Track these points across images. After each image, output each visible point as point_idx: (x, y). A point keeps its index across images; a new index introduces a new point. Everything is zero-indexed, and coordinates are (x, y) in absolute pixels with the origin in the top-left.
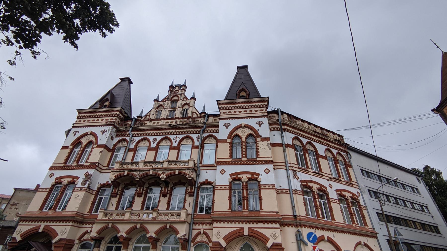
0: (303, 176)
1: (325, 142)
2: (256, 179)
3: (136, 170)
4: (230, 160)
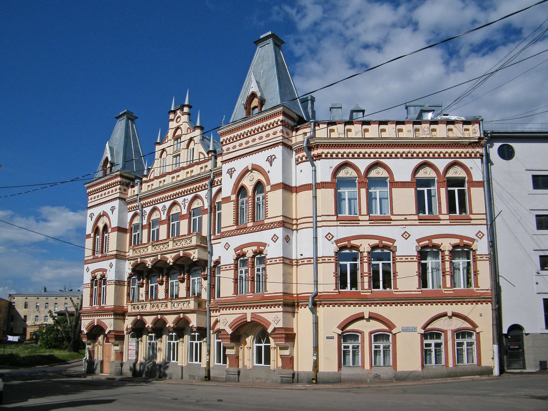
0: (344, 232)
2: (261, 252)
4: (235, 227)
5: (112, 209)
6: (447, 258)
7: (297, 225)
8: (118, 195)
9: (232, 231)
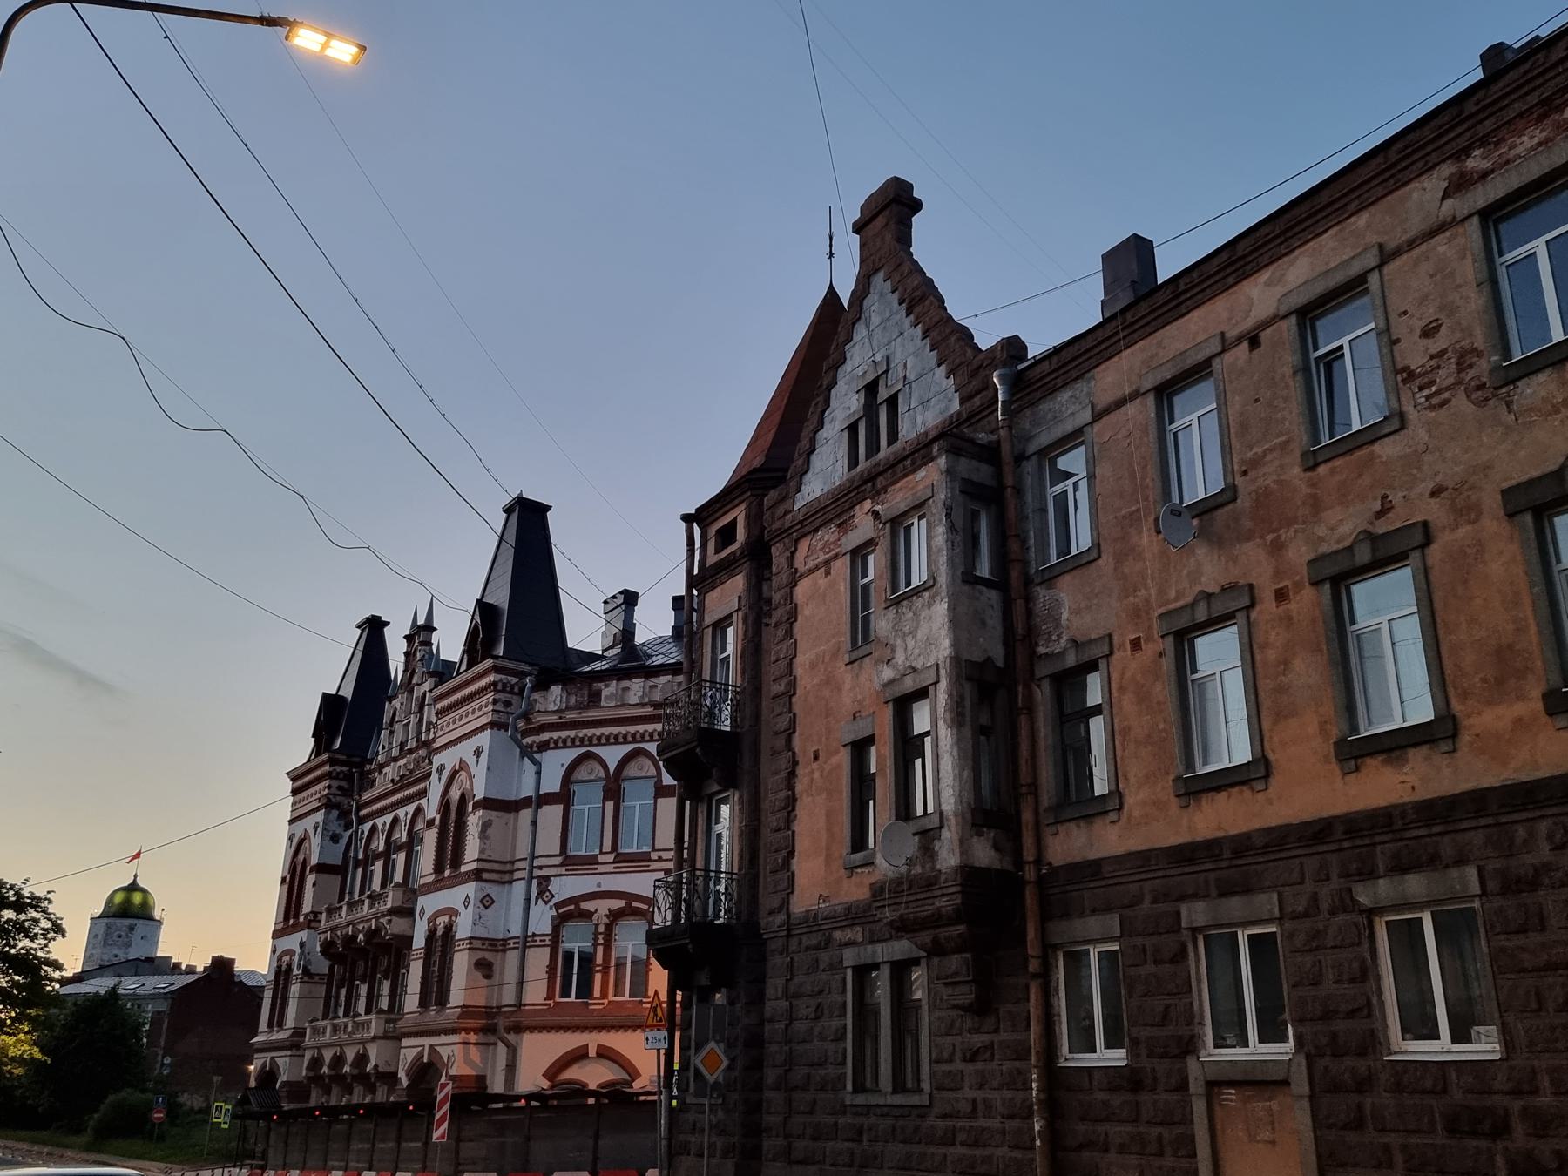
0: (567, 887)
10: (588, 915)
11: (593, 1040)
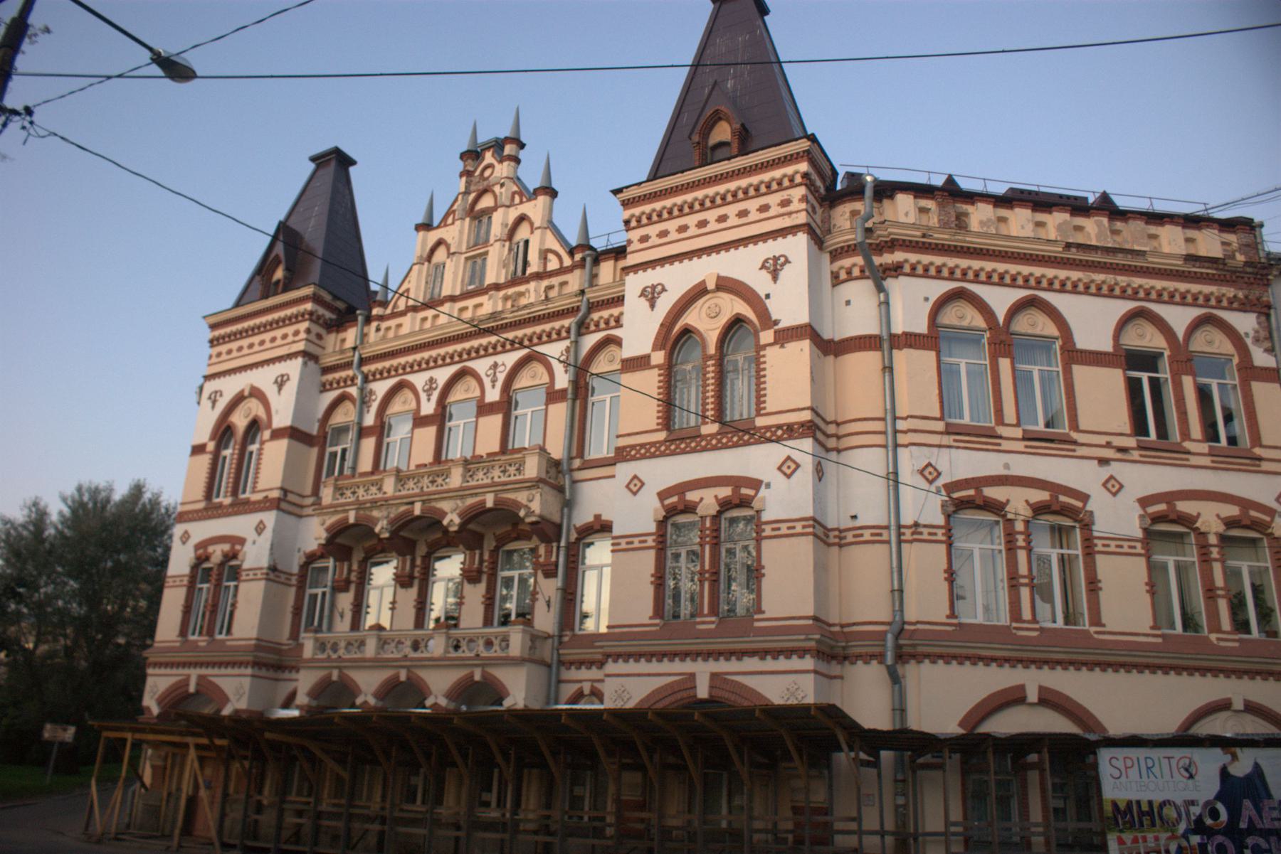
0: (966, 464)
1: (1123, 280)
2: (745, 503)
3: (375, 504)
5: (281, 383)
6: (1215, 553)
7: (838, 437)
8: (301, 346)
9: (652, 444)
10: (996, 508)
11: (1032, 680)
